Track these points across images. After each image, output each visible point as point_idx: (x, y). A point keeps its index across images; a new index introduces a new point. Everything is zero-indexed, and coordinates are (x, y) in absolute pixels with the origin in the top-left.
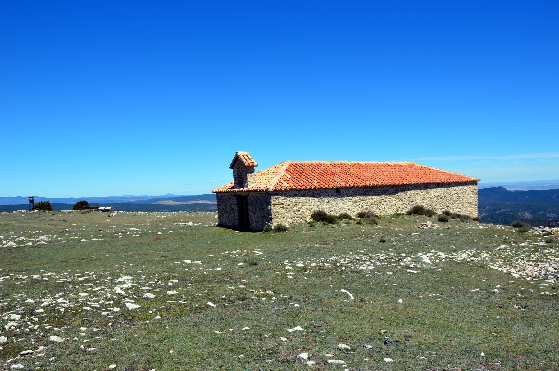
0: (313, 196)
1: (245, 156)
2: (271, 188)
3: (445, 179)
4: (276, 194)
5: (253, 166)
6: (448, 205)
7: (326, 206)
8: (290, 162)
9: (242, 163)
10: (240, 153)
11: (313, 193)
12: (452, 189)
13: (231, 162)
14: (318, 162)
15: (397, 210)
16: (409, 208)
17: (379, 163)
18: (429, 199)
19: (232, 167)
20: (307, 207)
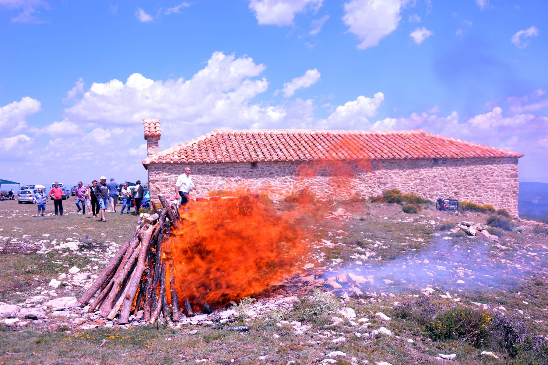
0: (213, 173)
1: (152, 125)
4: (157, 168)
5: (159, 136)
6: (456, 190)
11: (213, 169)
15: (357, 194)
16: (379, 192)
17: (364, 133)
18: (418, 181)
20: (204, 186)
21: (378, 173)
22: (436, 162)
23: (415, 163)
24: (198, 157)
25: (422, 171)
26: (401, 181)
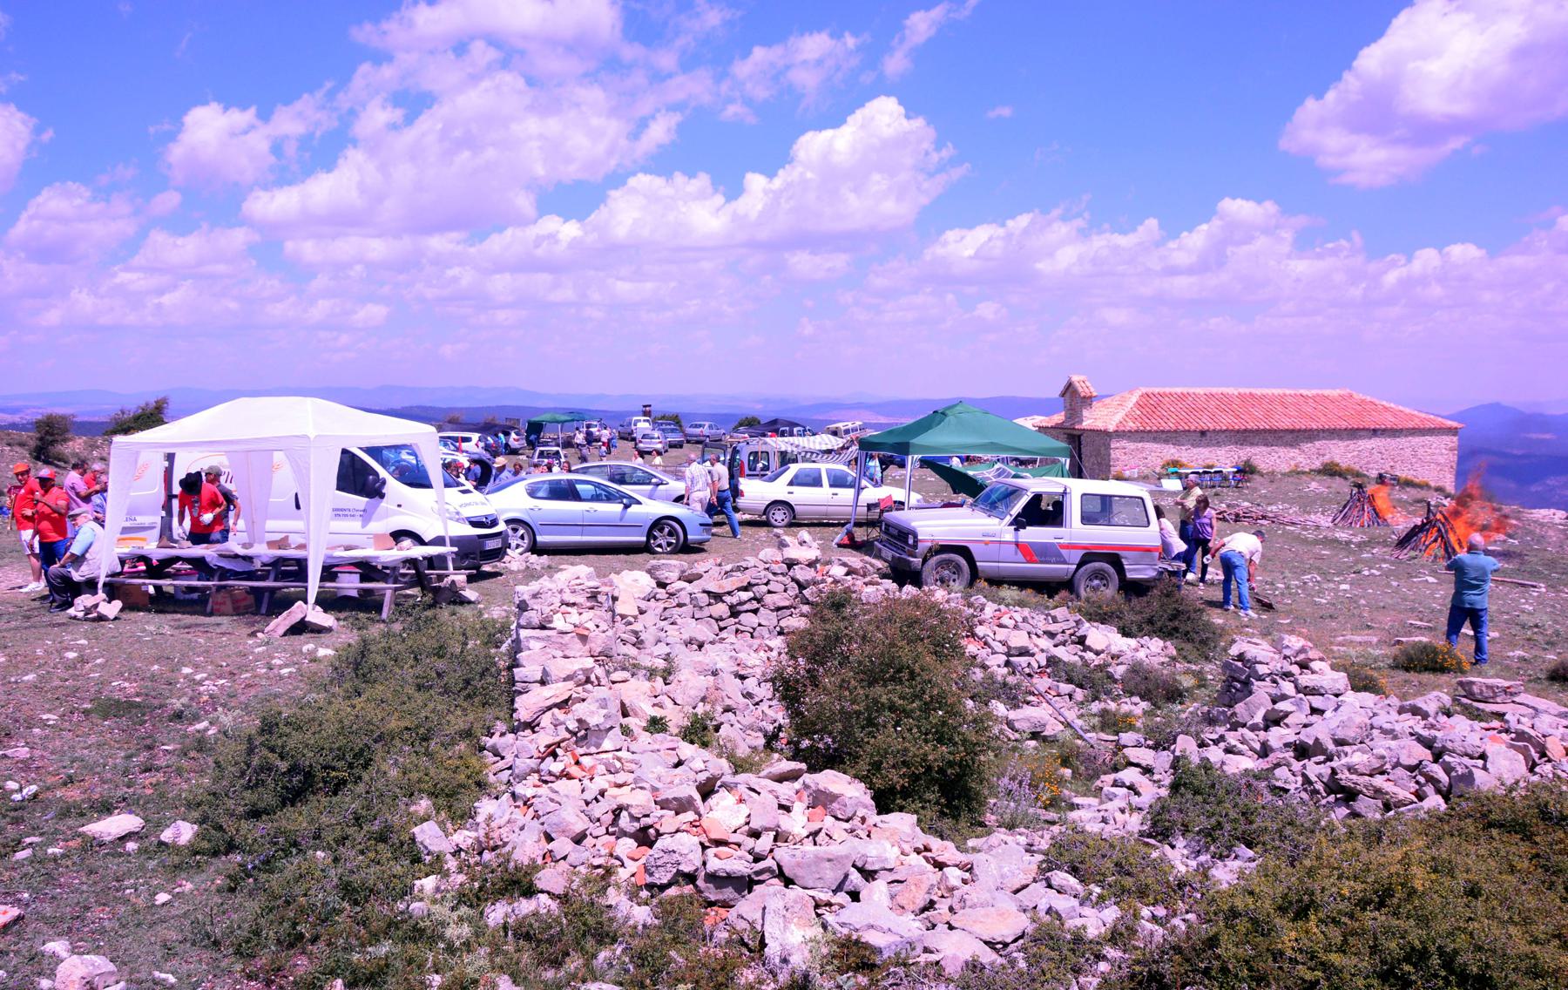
0: (1166, 441)
2: (1111, 428)
3: (1389, 421)
8: (1144, 390)
9: (1075, 392)
10: (1075, 379)
12: (1402, 441)
13: (1061, 388)
14: (1185, 390)
16: (1317, 464)
19: (1063, 395)
22: (1375, 432)
23: (1353, 433)
24: (1151, 425)
26: (1340, 453)
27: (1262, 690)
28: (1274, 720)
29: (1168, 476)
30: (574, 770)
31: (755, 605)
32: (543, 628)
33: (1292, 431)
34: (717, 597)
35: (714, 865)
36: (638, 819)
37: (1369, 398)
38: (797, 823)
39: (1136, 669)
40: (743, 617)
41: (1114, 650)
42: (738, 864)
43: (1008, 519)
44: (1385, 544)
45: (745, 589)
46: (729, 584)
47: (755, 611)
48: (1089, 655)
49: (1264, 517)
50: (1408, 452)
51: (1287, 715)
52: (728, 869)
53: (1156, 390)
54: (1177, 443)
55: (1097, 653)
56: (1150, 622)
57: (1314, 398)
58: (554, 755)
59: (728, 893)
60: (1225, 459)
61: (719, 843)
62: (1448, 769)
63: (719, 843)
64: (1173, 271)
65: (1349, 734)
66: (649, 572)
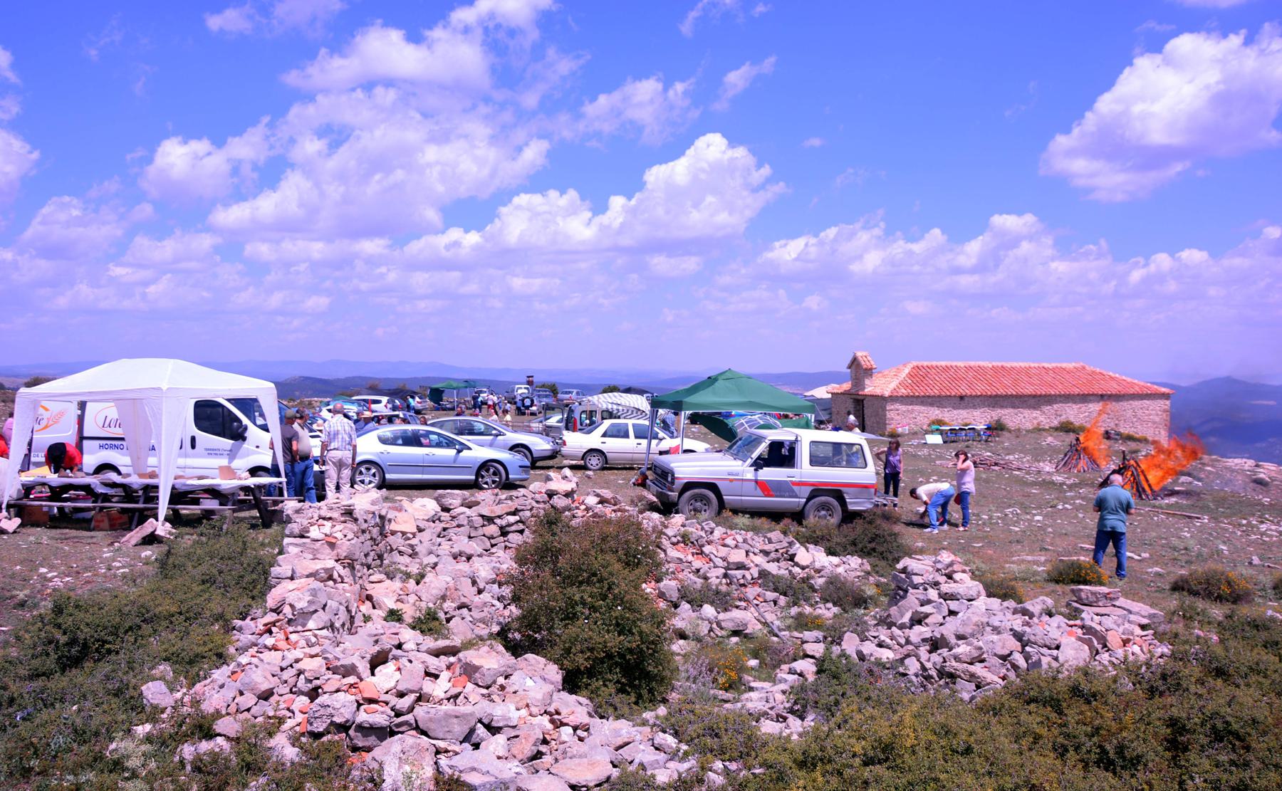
0: (932, 405)
2: (887, 394)
7: (947, 415)
8: (915, 364)
9: (859, 365)
10: (859, 354)
12: (1125, 404)
13: (848, 362)
14: (949, 364)
16: (1056, 423)
19: (849, 367)
21: (1055, 406)
23: (1084, 398)
24: (919, 392)
25: (1090, 405)
26: (1074, 413)
27: (913, 597)
28: (918, 620)
29: (932, 432)
30: (282, 644)
31: (521, 526)
32: (302, 536)
33: (1034, 396)
34: (490, 520)
35: (362, 717)
36: (311, 681)
37: (1098, 370)
38: (439, 688)
39: (833, 581)
40: (510, 536)
41: (818, 565)
42: (379, 717)
43: (749, 461)
44: (1092, 485)
45: (514, 513)
46: (499, 510)
47: (521, 532)
48: (796, 570)
49: (996, 464)
50: (1129, 413)
51: (927, 616)
52: (371, 720)
53: (925, 364)
54: (941, 406)
55: (803, 568)
56: (854, 543)
57: (1054, 370)
58: (270, 632)
59: (372, 740)
60: (979, 419)
61: (371, 701)
62: (1027, 657)
63: (371, 701)
64: (958, 271)
65: (968, 630)
66: (436, 499)
